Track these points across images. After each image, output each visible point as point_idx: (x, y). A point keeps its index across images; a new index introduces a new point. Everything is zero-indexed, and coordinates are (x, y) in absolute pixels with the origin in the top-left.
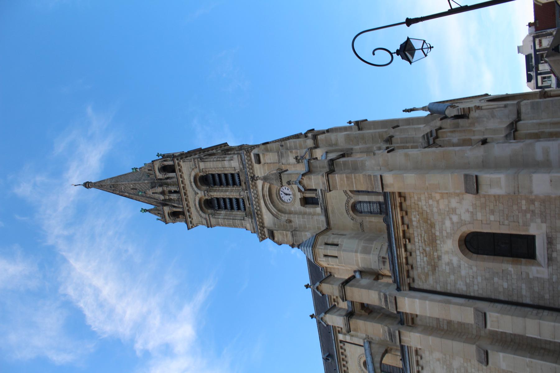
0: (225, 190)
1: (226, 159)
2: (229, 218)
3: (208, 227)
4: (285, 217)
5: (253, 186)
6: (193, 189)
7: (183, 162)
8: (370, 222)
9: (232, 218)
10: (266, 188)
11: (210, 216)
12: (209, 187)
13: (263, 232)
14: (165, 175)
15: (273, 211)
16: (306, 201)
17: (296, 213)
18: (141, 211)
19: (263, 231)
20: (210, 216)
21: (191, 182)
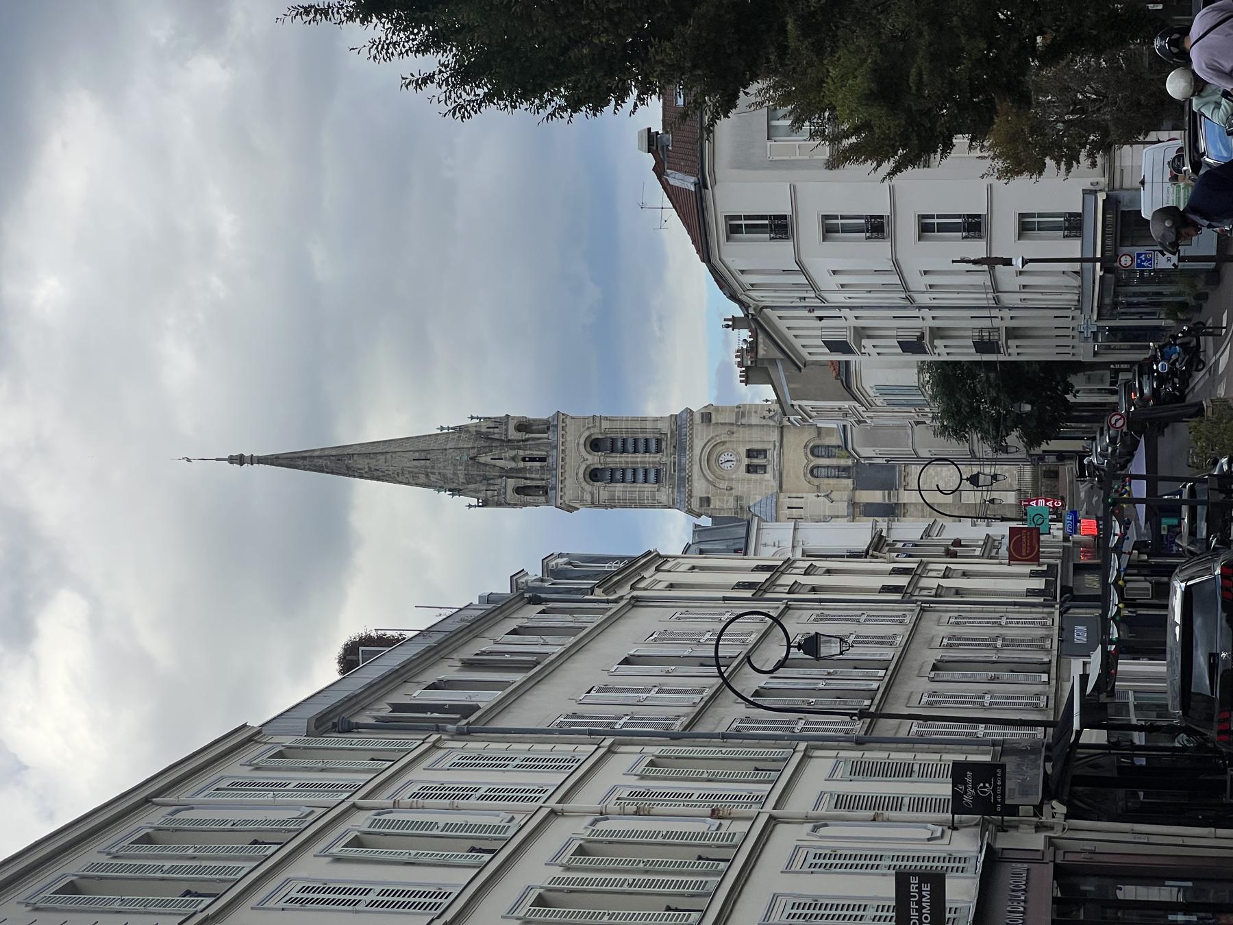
8: (829, 484)
16: (750, 469)
17: (737, 481)
21: (578, 445)
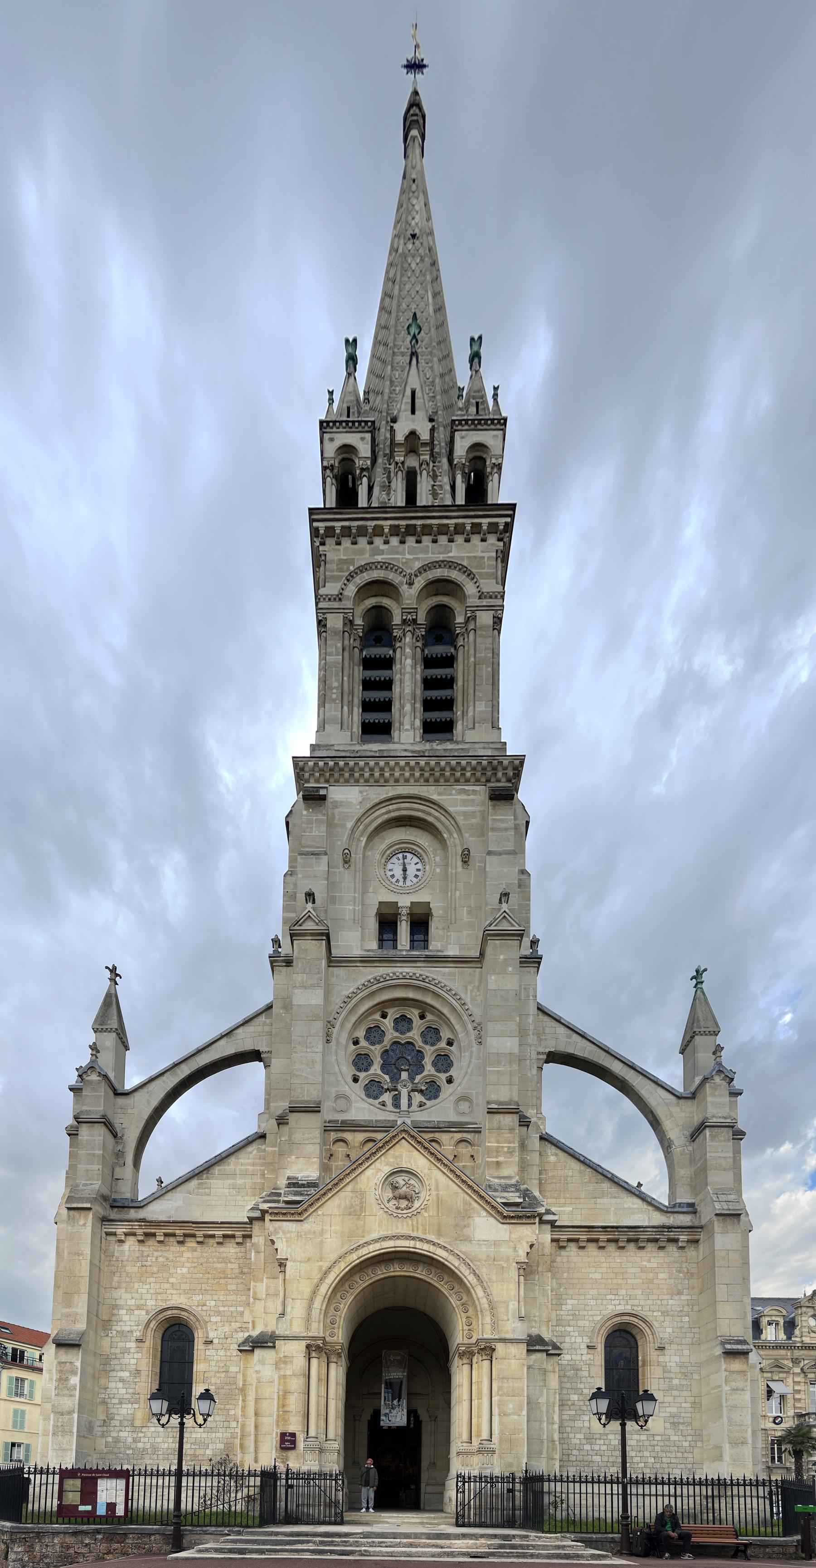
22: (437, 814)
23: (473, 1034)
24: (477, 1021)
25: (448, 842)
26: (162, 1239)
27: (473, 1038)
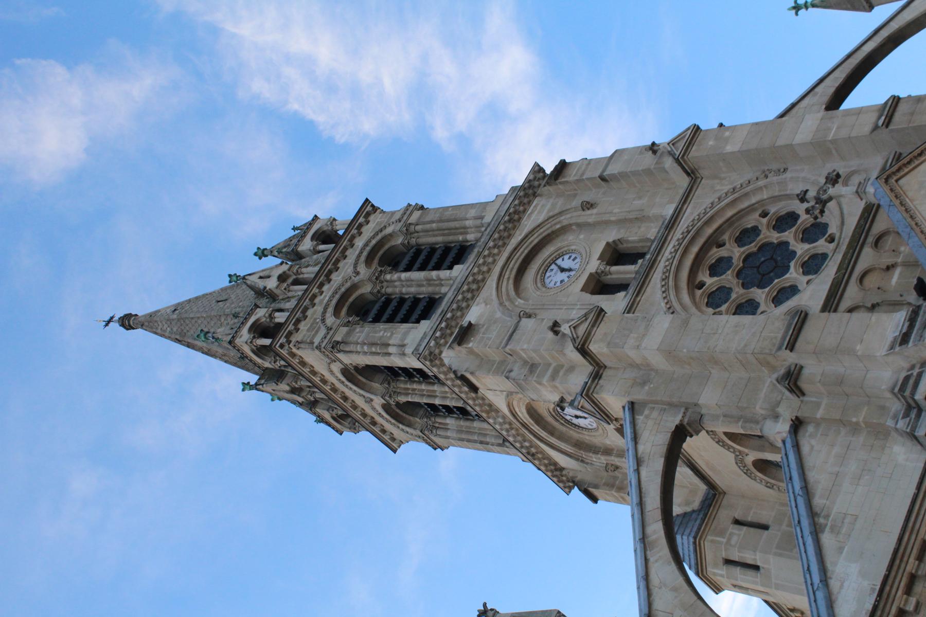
0: (428, 391)
1: (391, 350)
2: (470, 437)
3: (435, 449)
4: (599, 459)
5: (488, 412)
6: (355, 391)
7: (298, 349)
9: (476, 438)
10: (522, 413)
11: (426, 432)
12: (389, 384)
13: (564, 478)
14: (275, 362)
15: (562, 447)
18: (272, 400)
19: (562, 476)
20: (426, 432)
22: (535, 236)
23: (773, 178)
24: (758, 174)
25: (564, 224)
26: (913, 601)
27: (775, 178)
